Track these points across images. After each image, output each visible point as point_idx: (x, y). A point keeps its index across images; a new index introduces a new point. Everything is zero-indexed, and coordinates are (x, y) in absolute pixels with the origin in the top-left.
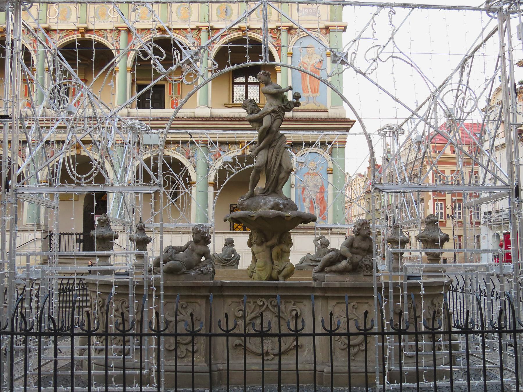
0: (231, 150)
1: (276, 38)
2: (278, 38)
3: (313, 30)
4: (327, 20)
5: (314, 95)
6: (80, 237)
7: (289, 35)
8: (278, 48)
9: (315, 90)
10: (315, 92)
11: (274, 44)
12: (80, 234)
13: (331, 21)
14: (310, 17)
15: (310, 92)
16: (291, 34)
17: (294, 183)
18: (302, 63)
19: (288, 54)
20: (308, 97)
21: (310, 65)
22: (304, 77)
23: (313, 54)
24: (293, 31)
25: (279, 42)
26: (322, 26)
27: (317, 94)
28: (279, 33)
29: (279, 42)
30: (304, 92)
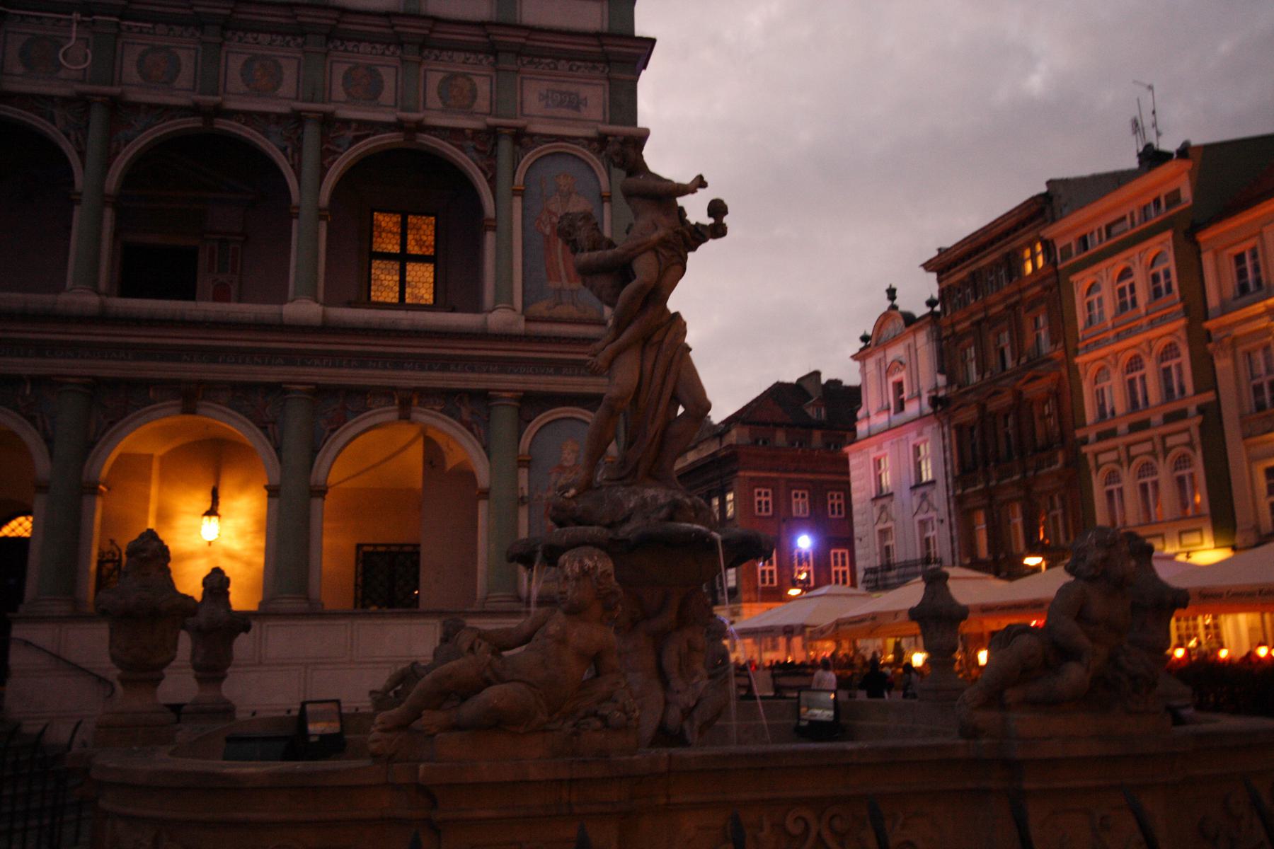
0: (370, 409)
4: (603, 122)
7: (517, 148)
13: (612, 122)
14: (564, 112)
15: (565, 281)
16: (521, 145)
20: (560, 291)
23: (570, 194)
24: (525, 140)
26: (591, 133)
28: (492, 141)
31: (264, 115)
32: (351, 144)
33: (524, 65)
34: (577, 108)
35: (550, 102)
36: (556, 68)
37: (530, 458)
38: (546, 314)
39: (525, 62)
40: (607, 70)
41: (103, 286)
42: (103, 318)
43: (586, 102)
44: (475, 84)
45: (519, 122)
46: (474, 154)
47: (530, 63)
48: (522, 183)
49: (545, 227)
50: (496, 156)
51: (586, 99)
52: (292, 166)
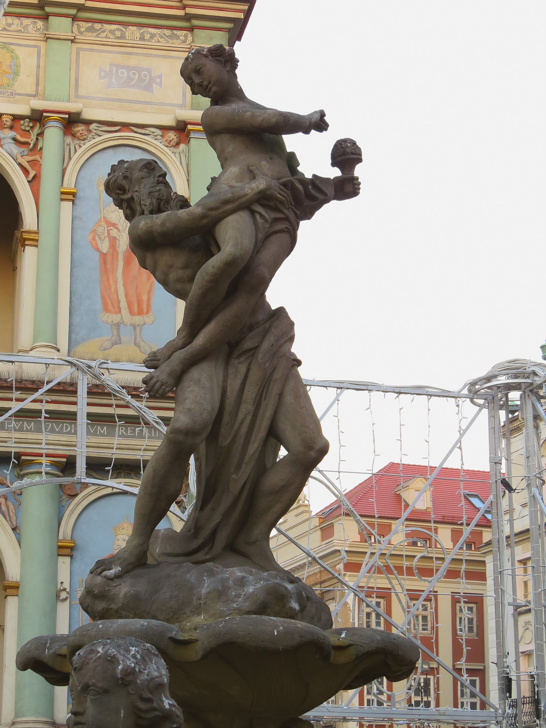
1: (28, 144)
2: (35, 145)
3: (139, 130)
4: (182, 106)
5: (137, 319)
7: (69, 139)
8: (32, 174)
9: (139, 305)
11: (20, 160)
14: (133, 93)
15: (125, 312)
16: (74, 136)
17: (67, 585)
18: (103, 223)
19: (62, 193)
20: (118, 325)
22: (109, 266)
24: (80, 128)
25: (37, 157)
26: (168, 120)
27: (147, 319)
28: (36, 130)
29: (37, 157)
30: (106, 309)
33: (81, 33)
34: (148, 88)
35: (114, 80)
36: (123, 37)
37: (73, 544)
39: (82, 29)
40: (190, 39)
43: (161, 81)
44: (17, 57)
45: (73, 107)
47: (89, 30)
48: (73, 186)
49: (102, 240)
50: (41, 149)
51: (160, 77)
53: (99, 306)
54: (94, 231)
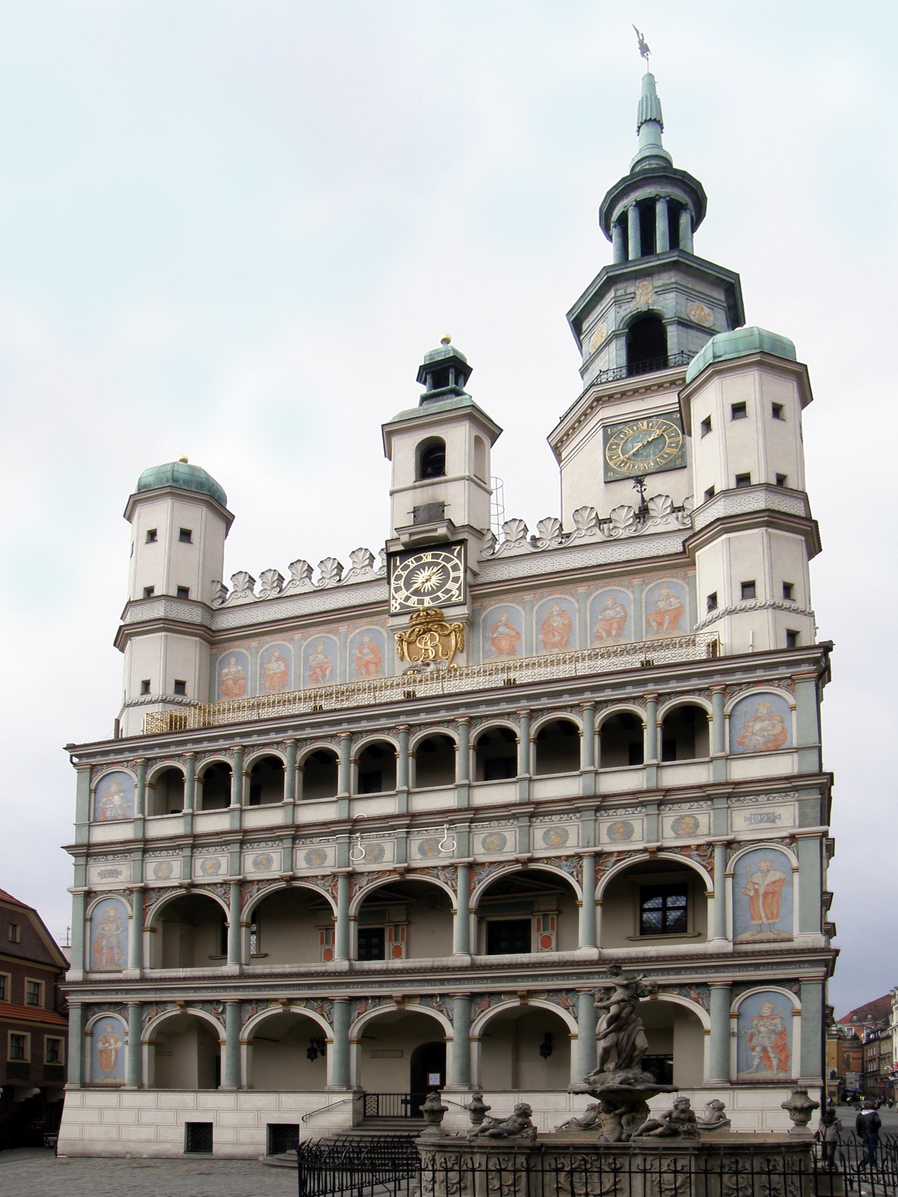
5: (771, 921)
6: (406, 1097)
10: (773, 918)
12: (406, 1095)
16: (731, 849)
20: (760, 925)
21: (765, 884)
23: (768, 871)
28: (711, 849)
31: (559, 857)
32: (614, 864)
38: (750, 938)
41: (473, 949)
42: (473, 967)
46: (699, 859)
49: (750, 891)
52: (577, 881)
53: (749, 918)
54: (746, 888)
